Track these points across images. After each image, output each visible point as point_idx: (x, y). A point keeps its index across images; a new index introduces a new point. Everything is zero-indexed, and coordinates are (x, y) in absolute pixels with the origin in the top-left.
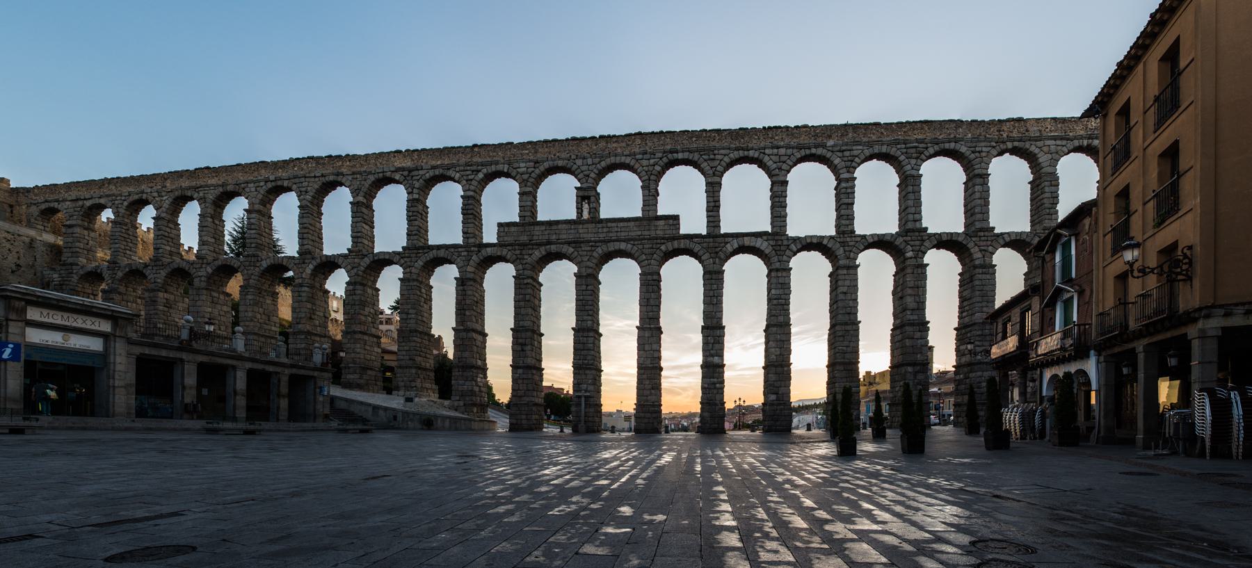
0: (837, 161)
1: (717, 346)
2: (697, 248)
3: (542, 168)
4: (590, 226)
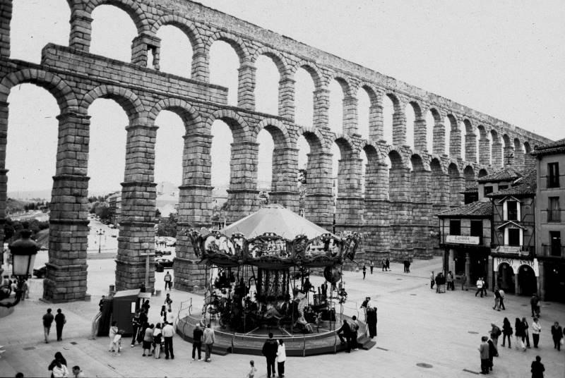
0: (320, 75)
2: (240, 120)
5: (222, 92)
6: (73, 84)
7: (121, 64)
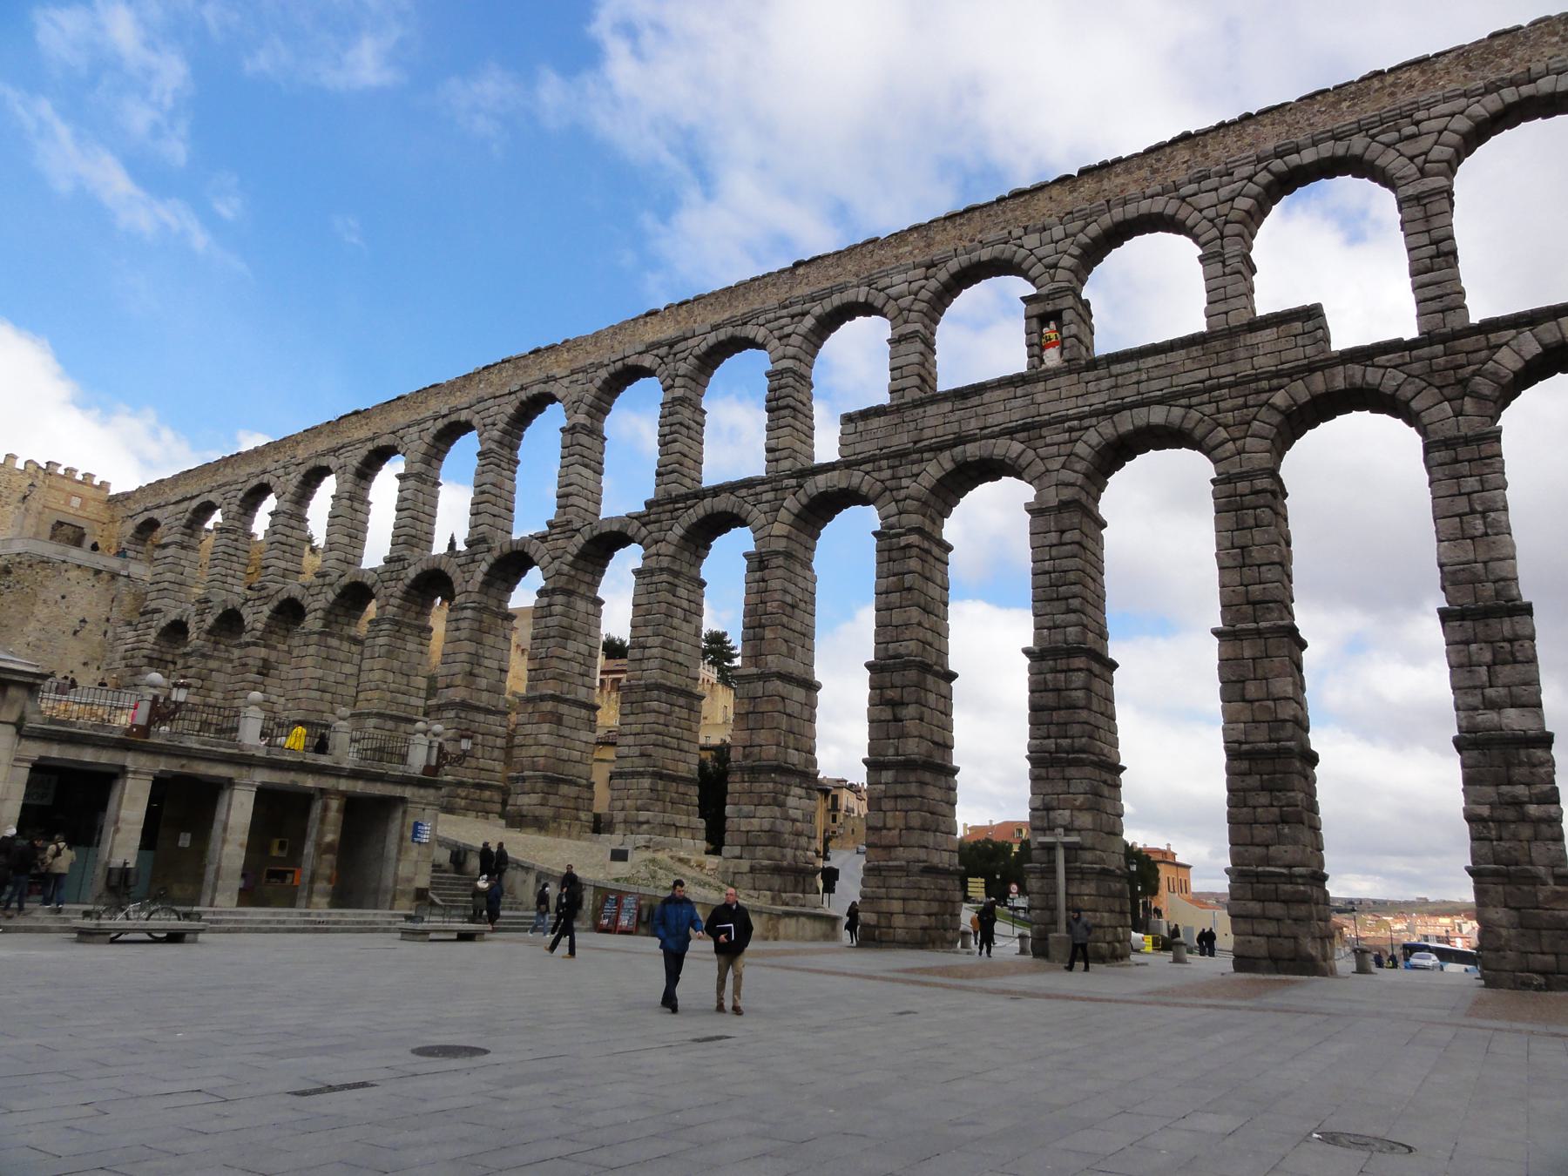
1: (1506, 672)
2: (1391, 381)
3: (943, 275)
4: (1063, 381)
5: (1297, 326)
6: (887, 474)
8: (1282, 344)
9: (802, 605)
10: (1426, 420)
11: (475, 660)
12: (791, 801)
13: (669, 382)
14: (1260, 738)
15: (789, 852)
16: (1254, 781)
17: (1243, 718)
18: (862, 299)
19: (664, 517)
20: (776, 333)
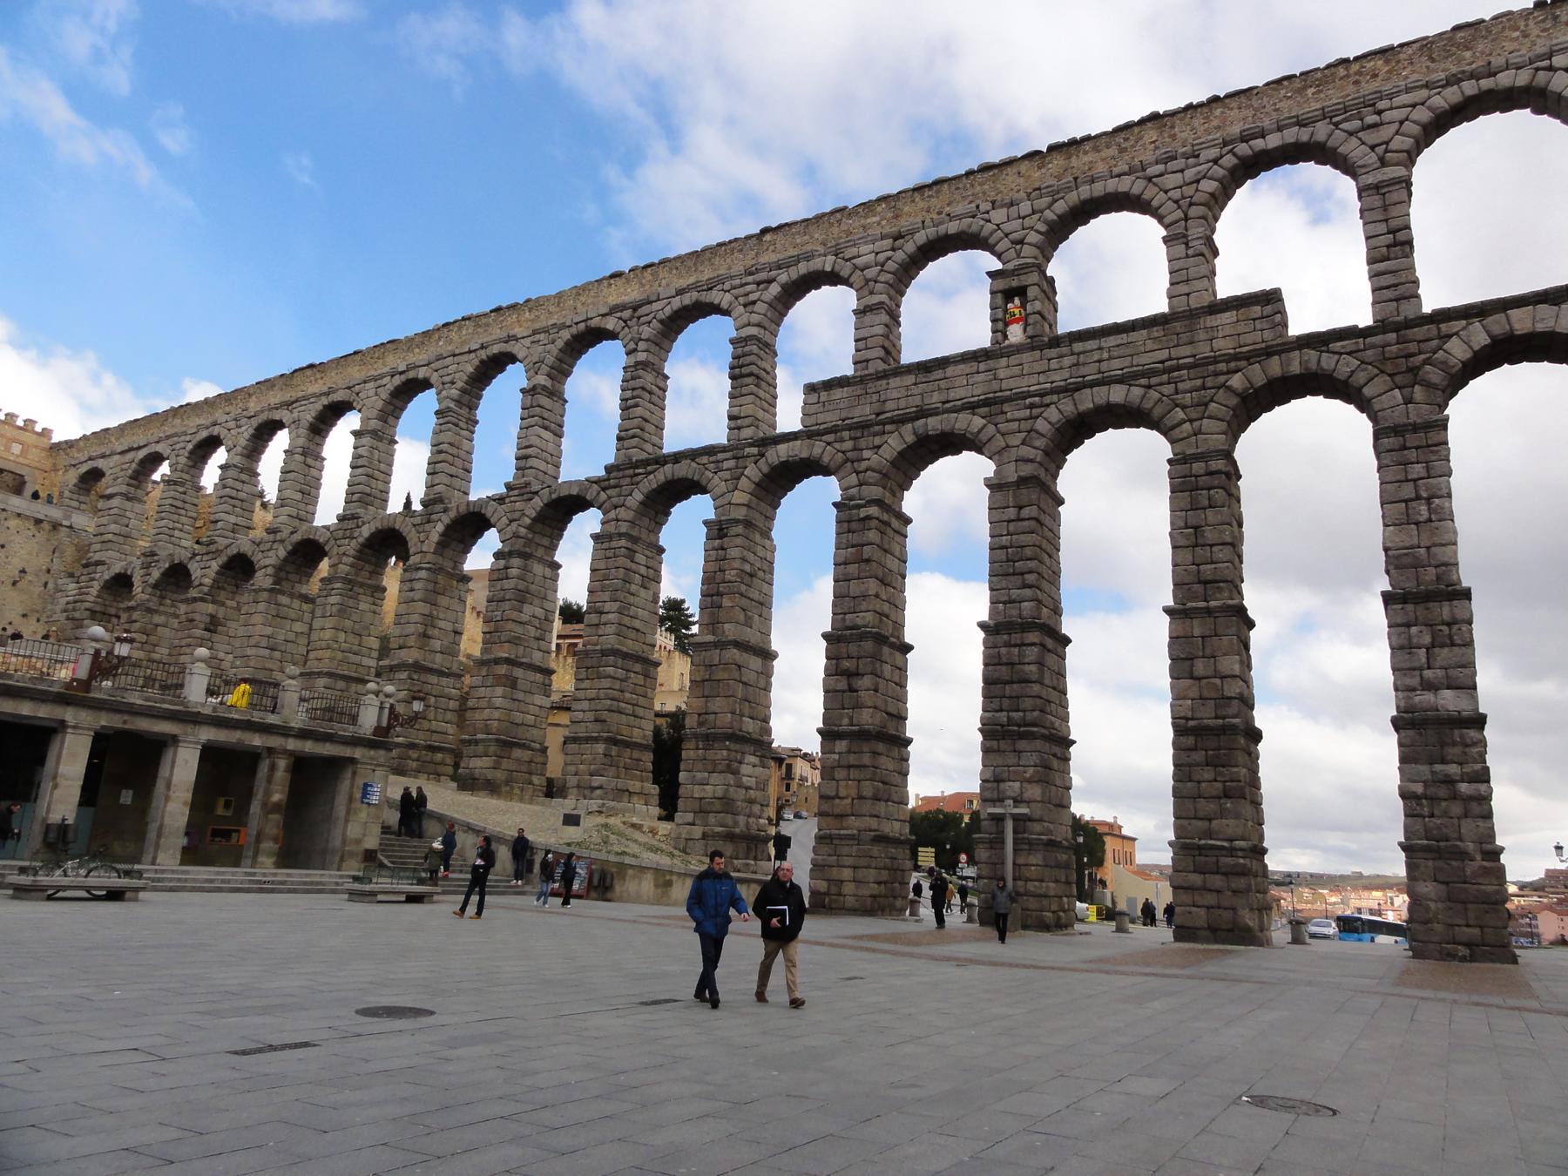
1: (1443, 655)
2: (1345, 367)
3: (910, 247)
4: (1026, 357)
5: (1256, 310)
6: (849, 445)
7: (942, 363)
8: (1241, 328)
9: (761, 574)
10: (1377, 407)
11: (429, 620)
12: (745, 769)
13: (632, 346)
14: (1207, 716)
15: (742, 819)
16: (1199, 756)
17: (1191, 695)
18: (828, 269)
19: (623, 482)
20: (741, 300)
